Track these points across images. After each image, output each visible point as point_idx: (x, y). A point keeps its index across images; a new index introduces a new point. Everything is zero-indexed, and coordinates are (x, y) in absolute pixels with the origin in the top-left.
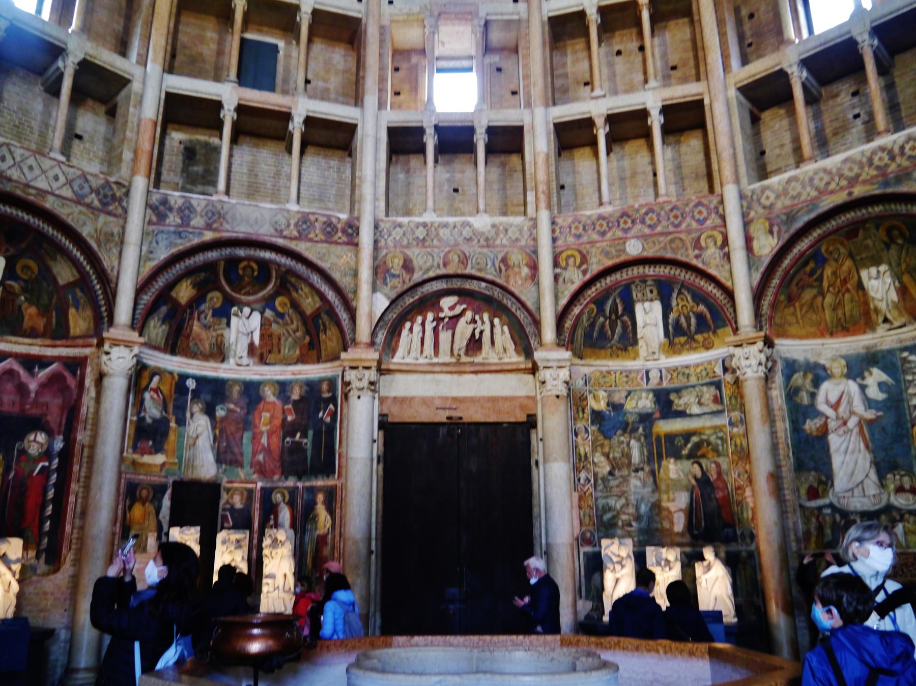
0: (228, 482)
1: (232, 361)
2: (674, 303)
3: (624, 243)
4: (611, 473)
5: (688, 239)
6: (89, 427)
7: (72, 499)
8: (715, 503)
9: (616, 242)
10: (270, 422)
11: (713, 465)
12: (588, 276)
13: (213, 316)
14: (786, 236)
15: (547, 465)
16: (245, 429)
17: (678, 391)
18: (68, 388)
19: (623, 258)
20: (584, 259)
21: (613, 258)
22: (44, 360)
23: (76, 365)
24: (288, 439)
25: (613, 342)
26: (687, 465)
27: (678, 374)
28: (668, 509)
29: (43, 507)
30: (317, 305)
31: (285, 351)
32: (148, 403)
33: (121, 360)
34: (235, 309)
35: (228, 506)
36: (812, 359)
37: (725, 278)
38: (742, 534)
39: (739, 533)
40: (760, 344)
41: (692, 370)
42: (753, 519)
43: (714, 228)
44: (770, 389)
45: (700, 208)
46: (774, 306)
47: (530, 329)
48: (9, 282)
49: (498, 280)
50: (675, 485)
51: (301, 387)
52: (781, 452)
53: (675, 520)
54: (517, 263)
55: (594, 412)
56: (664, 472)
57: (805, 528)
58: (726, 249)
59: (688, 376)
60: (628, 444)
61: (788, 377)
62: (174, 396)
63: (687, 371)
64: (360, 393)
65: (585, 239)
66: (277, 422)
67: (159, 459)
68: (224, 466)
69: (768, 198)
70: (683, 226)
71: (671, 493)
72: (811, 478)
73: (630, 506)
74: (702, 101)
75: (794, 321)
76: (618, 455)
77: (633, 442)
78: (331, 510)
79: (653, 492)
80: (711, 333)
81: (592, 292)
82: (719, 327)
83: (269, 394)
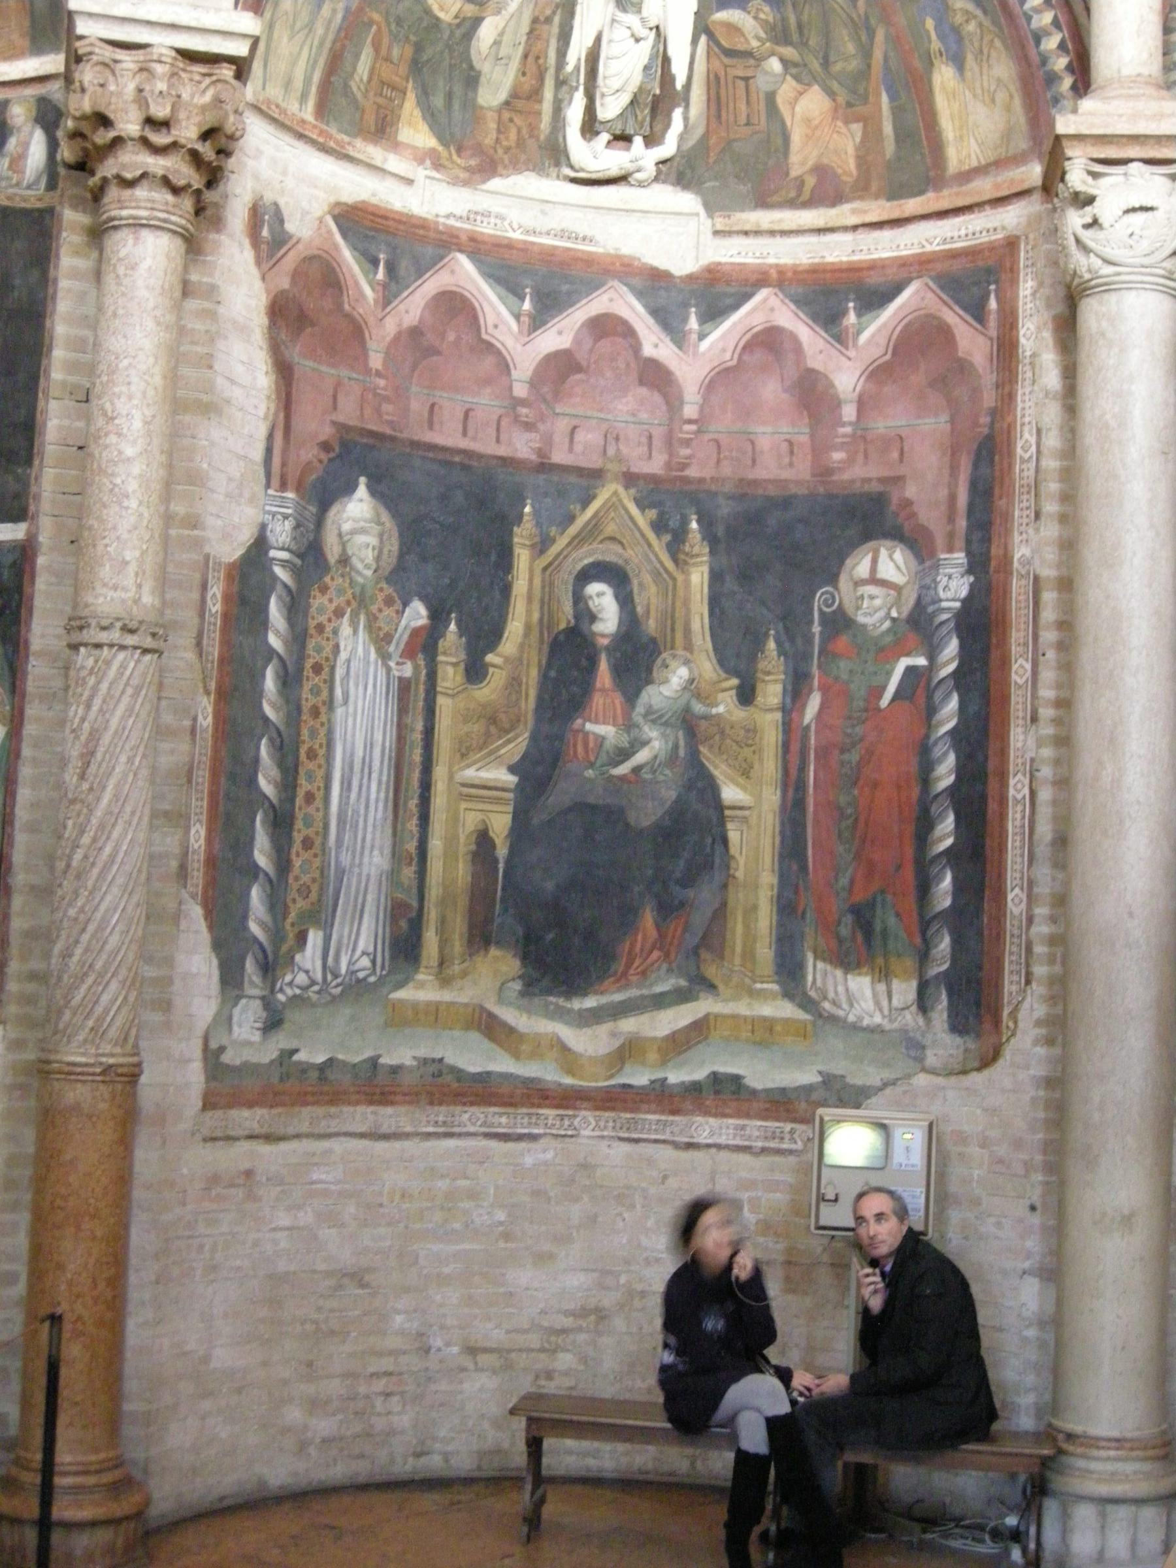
6: (1051, 507)
7: (1017, 787)
18: (963, 367)
22: (873, 279)
23: (976, 280)
29: (925, 825)
48: (721, 16)
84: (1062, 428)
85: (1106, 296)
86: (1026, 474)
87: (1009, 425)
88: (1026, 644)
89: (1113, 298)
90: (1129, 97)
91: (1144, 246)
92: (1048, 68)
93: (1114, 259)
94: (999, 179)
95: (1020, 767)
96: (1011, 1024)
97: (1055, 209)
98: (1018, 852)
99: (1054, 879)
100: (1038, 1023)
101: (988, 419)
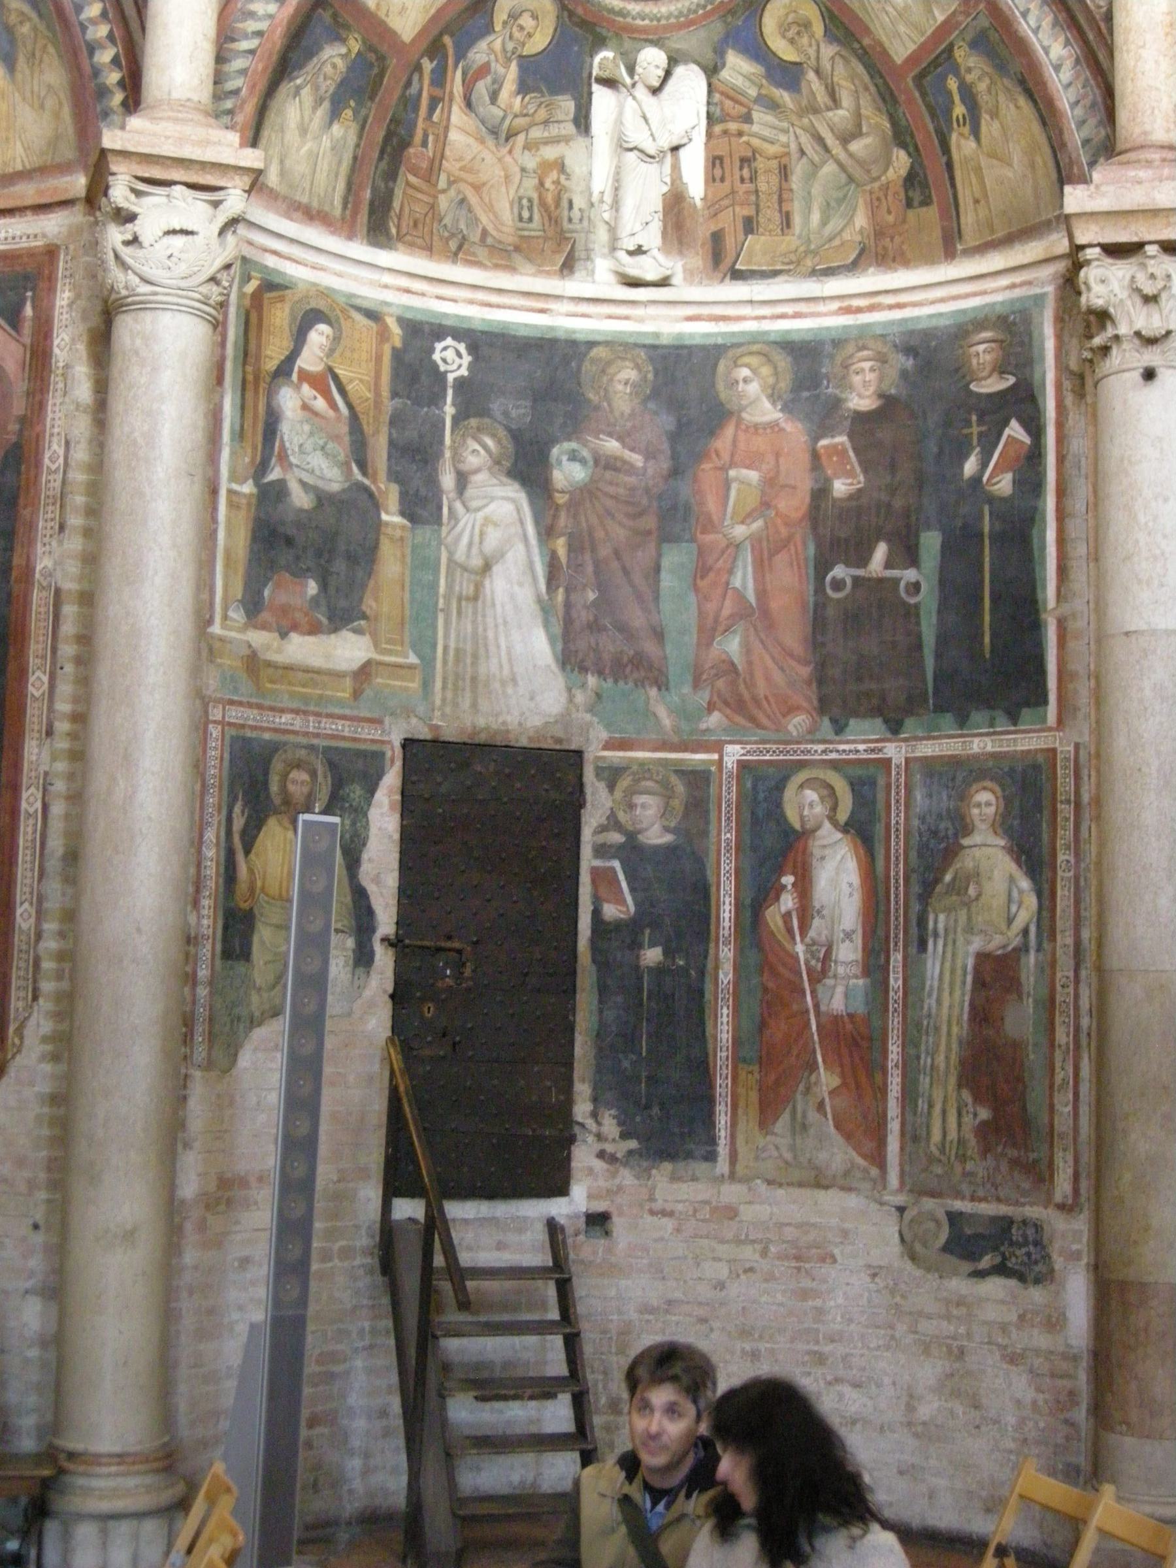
0: (608, 746)
1: (603, 267)
6: (75, 521)
7: (30, 800)
10: (766, 504)
13: (523, 88)
16: (666, 537)
24: (839, 571)
30: (940, 17)
31: (809, 219)
32: (293, 430)
33: (179, 241)
34: (605, 55)
35: (617, 838)
51: (882, 359)
62: (389, 406)
64: (1151, 357)
66: (794, 504)
67: (348, 650)
68: (592, 680)
78: (1032, 855)
83: (755, 394)
84: (90, 442)
85: (142, 314)
86: (52, 484)
87: (38, 436)
88: (44, 657)
89: (148, 316)
90: (176, 120)
91: (183, 269)
92: (101, 80)
93: (153, 279)
94: (43, 186)
95: (34, 781)
96: (17, 1041)
97: (96, 223)
98: (28, 866)
99: (64, 895)
100: (45, 1040)
101: (17, 427)
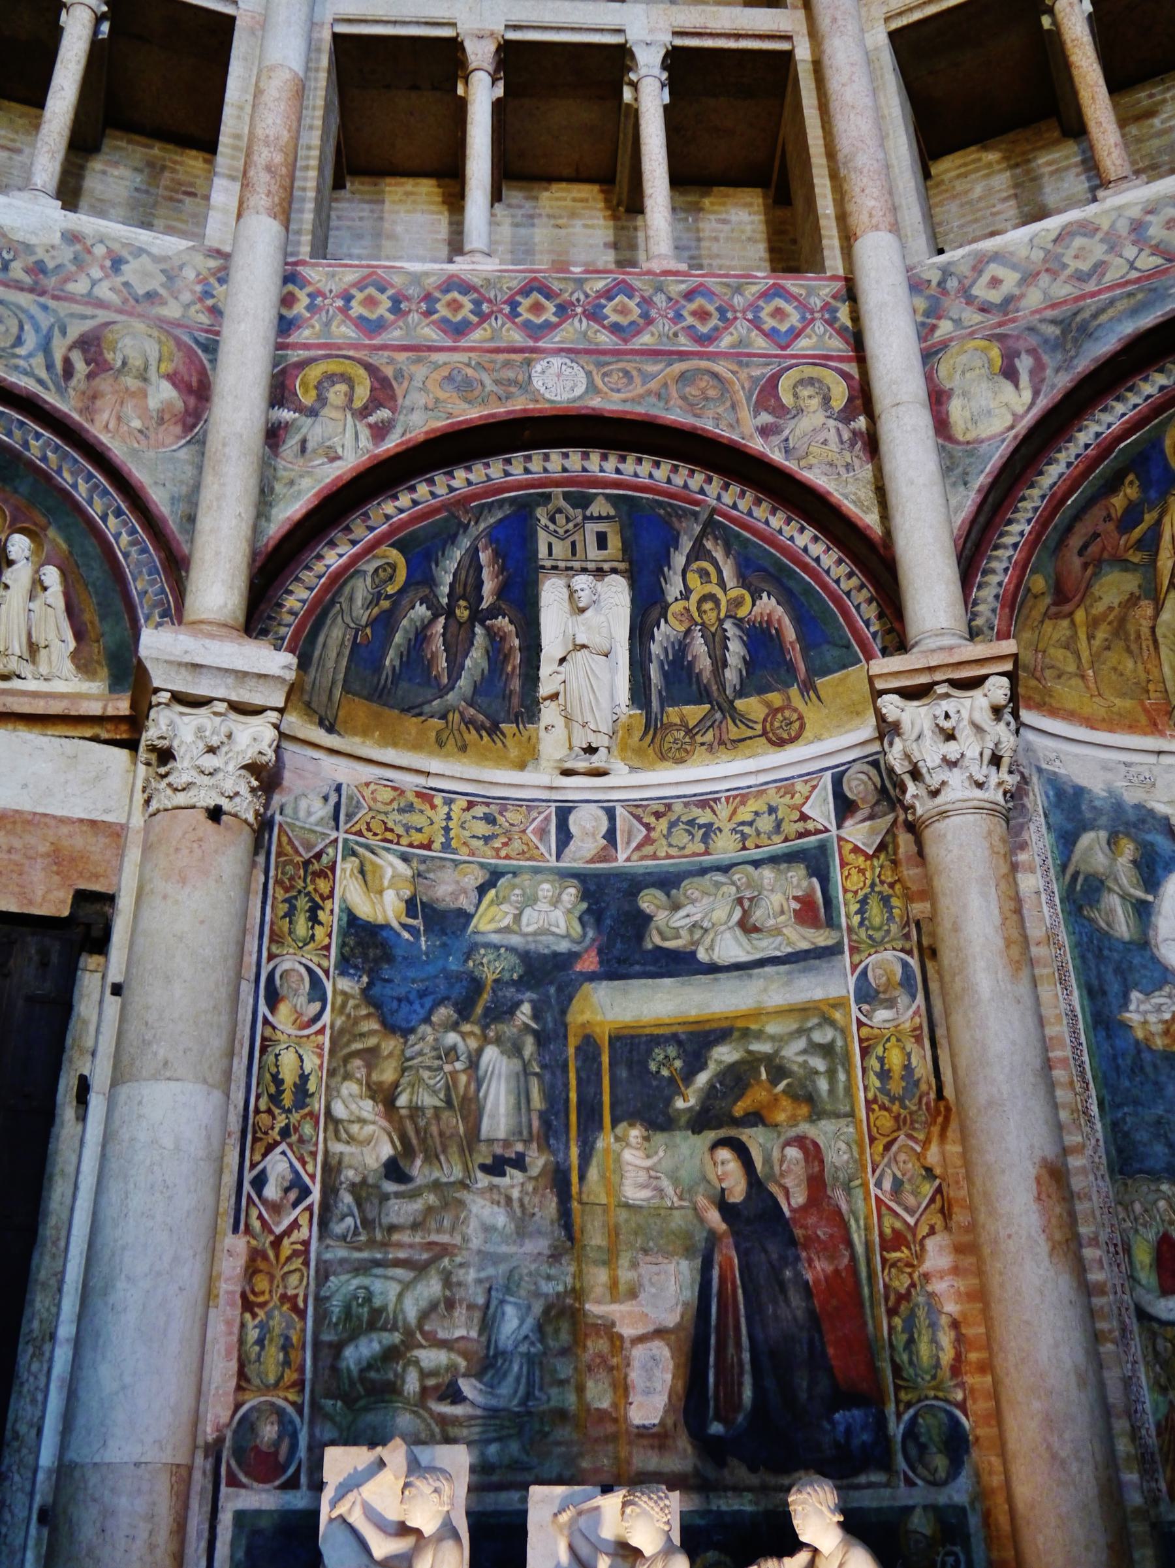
2: (673, 589)
3: (528, 363)
4: (394, 1170)
5: (742, 381)
8: (796, 1300)
9: (502, 357)
11: (793, 1152)
12: (391, 444)
14: (1060, 382)
15: (124, 1091)
17: (668, 882)
19: (519, 404)
20: (384, 391)
21: (484, 402)
25: (450, 697)
26: (690, 1150)
27: (672, 825)
28: (607, 1328)
36: (1132, 797)
37: (858, 502)
38: (911, 1433)
39: (897, 1429)
40: (998, 689)
41: (723, 810)
42: (956, 1369)
43: (822, 360)
44: (1014, 867)
45: (779, 302)
46: (1014, 602)
47: (144, 584)
49: (51, 398)
50: (644, 1232)
52: (1062, 1095)
53: (635, 1376)
54: (136, 362)
55: (352, 921)
56: (603, 1177)
57: (1163, 1409)
58: (861, 422)
59: (709, 831)
60: (473, 1063)
61: (1067, 840)
63: (705, 817)
65: (394, 335)
69: (995, 282)
70: (725, 342)
71: (624, 1261)
72: (1162, 1204)
73: (460, 1313)
74: (789, 55)
75: (1072, 668)
76: (428, 1100)
77: (491, 1053)
79: (555, 1257)
80: (794, 691)
81: (396, 508)
82: (826, 671)
